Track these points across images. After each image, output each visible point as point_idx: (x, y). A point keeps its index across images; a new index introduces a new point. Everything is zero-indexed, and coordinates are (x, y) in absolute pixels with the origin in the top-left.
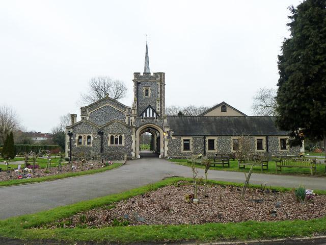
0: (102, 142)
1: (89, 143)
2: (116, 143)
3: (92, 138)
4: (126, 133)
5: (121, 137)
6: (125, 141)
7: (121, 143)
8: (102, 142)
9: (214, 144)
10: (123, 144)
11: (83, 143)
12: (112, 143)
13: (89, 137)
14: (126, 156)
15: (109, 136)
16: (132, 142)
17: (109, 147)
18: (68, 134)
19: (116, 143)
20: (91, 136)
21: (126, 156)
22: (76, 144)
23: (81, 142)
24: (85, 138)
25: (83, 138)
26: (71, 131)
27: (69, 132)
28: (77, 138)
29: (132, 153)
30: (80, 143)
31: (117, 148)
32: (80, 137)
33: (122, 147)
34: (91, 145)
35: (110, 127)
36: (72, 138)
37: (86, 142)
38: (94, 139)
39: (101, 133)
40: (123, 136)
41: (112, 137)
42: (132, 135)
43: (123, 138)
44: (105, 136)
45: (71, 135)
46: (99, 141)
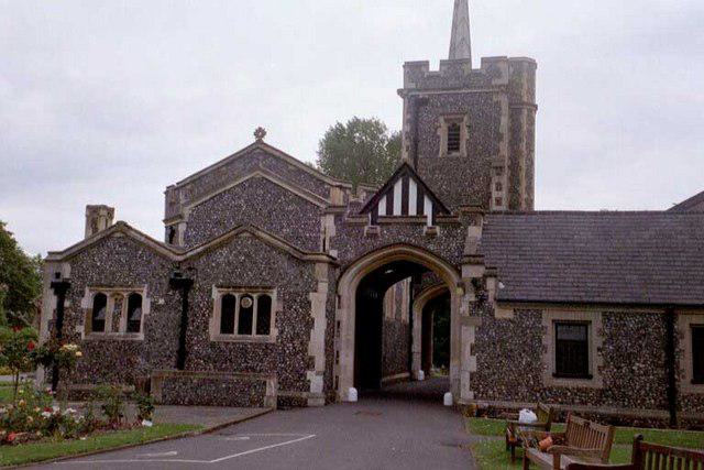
0: (184, 324)
1: (133, 326)
2: (245, 328)
3: (146, 307)
4: (285, 286)
5: (265, 303)
6: (284, 319)
7: (264, 328)
8: (184, 324)
9: (572, 377)
10: (274, 332)
11: (108, 326)
12: (226, 327)
13: (135, 301)
14: (272, 389)
15: (216, 295)
16: (310, 324)
17: (213, 345)
18: (53, 285)
19: (245, 328)
20: (144, 295)
21: (272, 389)
22: (80, 329)
23: (102, 322)
24: (118, 305)
25: (110, 303)
26: (66, 271)
27: (58, 275)
28: (87, 303)
29: (310, 375)
30: (98, 325)
31: (244, 351)
32: (100, 301)
33: (267, 347)
34: (141, 336)
35: (223, 256)
36: (67, 304)
37: (123, 322)
38: (155, 307)
39: (182, 285)
40: (274, 295)
41: (228, 302)
42: (312, 296)
43: (276, 306)
44: (196, 297)
45: (61, 288)
46: (175, 316)
